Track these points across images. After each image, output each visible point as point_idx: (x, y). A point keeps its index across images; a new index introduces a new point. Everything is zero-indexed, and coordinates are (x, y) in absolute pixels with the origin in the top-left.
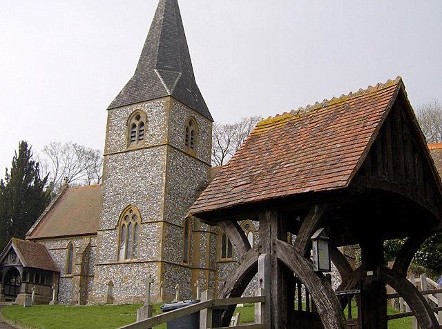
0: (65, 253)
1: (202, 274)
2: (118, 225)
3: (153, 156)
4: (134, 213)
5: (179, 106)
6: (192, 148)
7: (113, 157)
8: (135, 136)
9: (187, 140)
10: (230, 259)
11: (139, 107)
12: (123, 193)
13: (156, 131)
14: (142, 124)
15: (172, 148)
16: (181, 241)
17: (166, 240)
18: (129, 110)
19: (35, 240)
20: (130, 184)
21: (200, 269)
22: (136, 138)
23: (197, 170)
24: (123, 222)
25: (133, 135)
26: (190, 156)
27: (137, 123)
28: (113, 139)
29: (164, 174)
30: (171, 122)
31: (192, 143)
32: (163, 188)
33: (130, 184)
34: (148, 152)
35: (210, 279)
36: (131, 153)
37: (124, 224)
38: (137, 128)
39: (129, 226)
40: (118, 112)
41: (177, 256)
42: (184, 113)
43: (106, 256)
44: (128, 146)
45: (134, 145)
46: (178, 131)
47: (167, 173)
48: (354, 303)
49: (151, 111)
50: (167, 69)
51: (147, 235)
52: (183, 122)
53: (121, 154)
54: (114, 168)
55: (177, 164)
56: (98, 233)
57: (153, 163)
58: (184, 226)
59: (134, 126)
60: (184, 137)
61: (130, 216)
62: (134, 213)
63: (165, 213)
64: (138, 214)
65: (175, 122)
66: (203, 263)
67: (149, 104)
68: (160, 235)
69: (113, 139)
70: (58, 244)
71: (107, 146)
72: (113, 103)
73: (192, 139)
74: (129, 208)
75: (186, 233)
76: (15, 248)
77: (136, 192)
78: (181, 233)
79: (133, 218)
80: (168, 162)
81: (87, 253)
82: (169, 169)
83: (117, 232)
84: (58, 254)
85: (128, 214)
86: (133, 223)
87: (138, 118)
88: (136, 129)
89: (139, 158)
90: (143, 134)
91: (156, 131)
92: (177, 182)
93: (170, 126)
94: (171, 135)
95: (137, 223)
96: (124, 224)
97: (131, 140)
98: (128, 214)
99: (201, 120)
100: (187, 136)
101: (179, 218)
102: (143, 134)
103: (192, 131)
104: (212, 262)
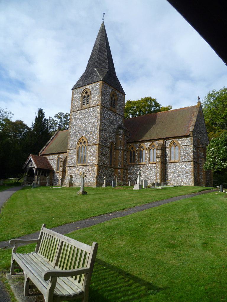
0: (56, 161)
1: (119, 171)
2: (77, 147)
3: (93, 111)
4: (84, 140)
5: (107, 86)
6: (114, 108)
7: (75, 113)
8: (85, 102)
9: (111, 104)
10: (134, 163)
11: (87, 87)
12: (79, 130)
13: (95, 99)
14: (88, 96)
15: (103, 107)
16: (108, 154)
17: (101, 154)
18: (82, 89)
19: (43, 155)
20: (82, 126)
22: (85, 103)
24: (79, 145)
25: (84, 101)
26: (113, 111)
27: (86, 96)
28: (75, 104)
29: (99, 120)
30: (103, 94)
31: (114, 105)
32: (99, 127)
33: (82, 126)
34: (91, 109)
35: (123, 174)
36: (83, 111)
38: (86, 98)
40: (77, 90)
41: (107, 162)
42: (110, 90)
43: (71, 162)
44: (82, 107)
45: (84, 106)
47: (100, 119)
48: (83, 275)
49: (93, 89)
50: (101, 68)
51: (90, 151)
53: (78, 111)
54: (75, 118)
55: (106, 115)
56: (68, 151)
57: (94, 115)
59: (85, 97)
60: (110, 102)
61: (83, 142)
62: (84, 140)
63: (99, 140)
64: (86, 141)
65: (105, 94)
66: (120, 166)
68: (97, 151)
69: (75, 104)
70: (53, 157)
71: (72, 108)
72: (75, 86)
73: (114, 103)
74: (82, 138)
75: (111, 150)
76: (32, 159)
77: (85, 130)
78: (108, 151)
79: (84, 143)
80: (101, 114)
81: (65, 161)
82: (102, 117)
83: (76, 150)
84: (53, 161)
85: (81, 141)
86: (84, 145)
87: (86, 93)
88: (86, 99)
89: (87, 113)
90: (89, 101)
91: (95, 99)
93: (102, 96)
94: (102, 100)
97: (83, 104)
99: (119, 94)
100: (111, 101)
101: (107, 143)
102: (89, 101)
103: (114, 100)
104: (125, 165)
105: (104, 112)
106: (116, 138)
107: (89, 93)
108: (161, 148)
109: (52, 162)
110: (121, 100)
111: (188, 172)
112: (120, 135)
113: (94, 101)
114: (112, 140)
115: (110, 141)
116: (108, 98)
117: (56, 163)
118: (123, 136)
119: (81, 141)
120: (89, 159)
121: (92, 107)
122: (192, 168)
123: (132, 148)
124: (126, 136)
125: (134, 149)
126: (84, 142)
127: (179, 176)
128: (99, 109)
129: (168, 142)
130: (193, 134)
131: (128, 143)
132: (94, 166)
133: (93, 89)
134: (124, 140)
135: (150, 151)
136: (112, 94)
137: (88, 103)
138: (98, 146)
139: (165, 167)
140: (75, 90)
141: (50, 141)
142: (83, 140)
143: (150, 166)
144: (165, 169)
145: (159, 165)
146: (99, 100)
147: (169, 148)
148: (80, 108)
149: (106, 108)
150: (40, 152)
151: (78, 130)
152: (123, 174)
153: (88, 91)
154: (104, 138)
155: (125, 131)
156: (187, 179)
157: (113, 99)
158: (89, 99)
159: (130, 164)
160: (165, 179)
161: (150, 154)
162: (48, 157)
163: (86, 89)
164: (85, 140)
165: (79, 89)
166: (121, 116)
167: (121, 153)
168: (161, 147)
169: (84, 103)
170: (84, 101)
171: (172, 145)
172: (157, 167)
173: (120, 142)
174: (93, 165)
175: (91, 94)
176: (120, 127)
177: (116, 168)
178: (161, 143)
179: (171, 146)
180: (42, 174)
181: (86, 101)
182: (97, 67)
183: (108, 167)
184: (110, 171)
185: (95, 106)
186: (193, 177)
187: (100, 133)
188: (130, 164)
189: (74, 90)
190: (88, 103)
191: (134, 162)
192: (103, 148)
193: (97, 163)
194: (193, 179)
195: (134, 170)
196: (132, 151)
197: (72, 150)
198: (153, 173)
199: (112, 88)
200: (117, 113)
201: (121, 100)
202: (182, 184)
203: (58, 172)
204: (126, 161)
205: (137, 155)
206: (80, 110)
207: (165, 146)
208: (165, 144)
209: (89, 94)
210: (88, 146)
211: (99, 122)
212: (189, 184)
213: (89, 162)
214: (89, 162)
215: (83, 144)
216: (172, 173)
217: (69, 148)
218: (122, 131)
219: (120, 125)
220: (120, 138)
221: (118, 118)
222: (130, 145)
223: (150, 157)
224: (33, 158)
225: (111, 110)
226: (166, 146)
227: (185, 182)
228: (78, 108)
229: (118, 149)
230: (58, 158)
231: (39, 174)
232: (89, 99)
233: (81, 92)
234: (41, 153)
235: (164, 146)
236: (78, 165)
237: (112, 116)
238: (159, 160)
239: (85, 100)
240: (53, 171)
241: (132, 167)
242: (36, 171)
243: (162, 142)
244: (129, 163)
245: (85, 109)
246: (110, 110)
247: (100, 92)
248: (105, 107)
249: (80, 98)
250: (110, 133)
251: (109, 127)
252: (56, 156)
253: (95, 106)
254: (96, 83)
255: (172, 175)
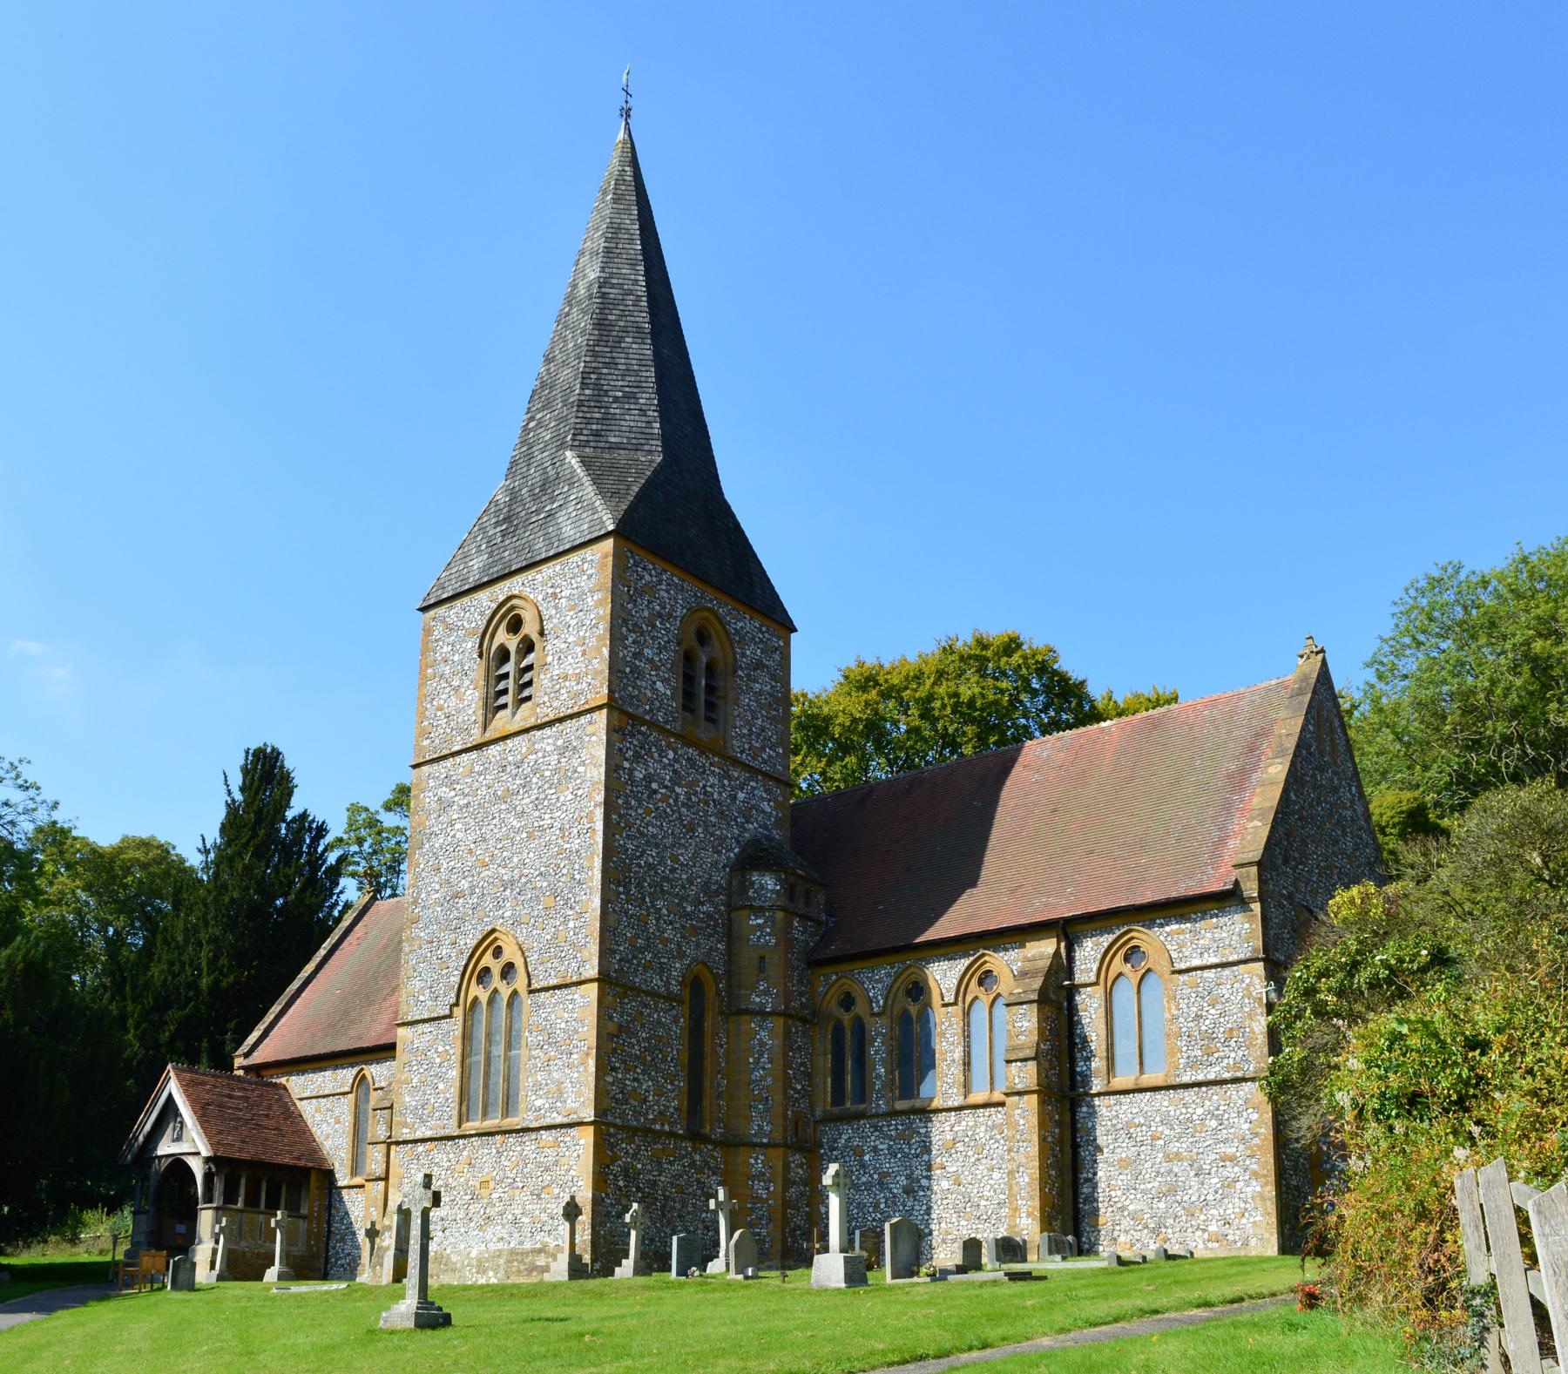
1: (757, 1162)
4: (507, 956)
5: (650, 572)
6: (714, 721)
8: (505, 692)
11: (514, 585)
12: (472, 888)
14: (528, 646)
16: (677, 1049)
18: (486, 601)
21: (755, 1145)
22: (508, 699)
23: (734, 798)
24: (476, 990)
25: (501, 686)
26: (703, 749)
27: (512, 643)
28: (440, 708)
30: (621, 624)
31: (710, 706)
34: (547, 740)
35: (787, 1183)
36: (494, 750)
37: (476, 998)
39: (491, 1001)
40: (451, 613)
44: (485, 728)
45: (503, 722)
46: (651, 661)
47: (609, 806)
52: (668, 631)
54: (445, 805)
55: (649, 778)
58: (687, 996)
59: (503, 655)
60: (677, 682)
61: (496, 967)
62: (507, 956)
63: (605, 953)
64: (519, 963)
65: (636, 628)
66: (759, 1125)
67: (547, 570)
69: (440, 708)
73: (710, 689)
74: (489, 942)
77: (512, 882)
83: (455, 1026)
86: (505, 992)
87: (515, 625)
88: (509, 667)
90: (529, 683)
91: (571, 665)
92: (652, 842)
94: (618, 672)
95: (515, 993)
96: (476, 998)
97: (492, 707)
98: (488, 960)
100: (689, 679)
101: (661, 970)
103: (710, 668)
105: (637, 757)
106: (730, 934)
107: (530, 628)
108: (1043, 992)
109: (318, 1117)
110: (759, 665)
111: (1232, 1159)
112: (759, 911)
113: (566, 678)
114: (698, 945)
115: (682, 955)
116: (659, 653)
117: (348, 1119)
118: (780, 915)
119: (488, 960)
120: (538, 1087)
121: (550, 724)
122: (1260, 1123)
123: (847, 1002)
124: (804, 918)
125: (860, 1009)
126: (508, 971)
127: (1172, 1191)
128: (595, 731)
129: (1089, 952)
130: (1262, 881)
131: (816, 961)
132: (574, 1132)
133: (554, 594)
134: (787, 942)
135: (967, 1014)
136: (692, 629)
137: (526, 693)
138: (592, 990)
139: (1074, 1122)
140: (441, 610)
141: (309, 968)
142: (498, 952)
143: (968, 1118)
144: (1074, 1137)
145: (1026, 1113)
146: (597, 673)
147: (1100, 990)
148: (476, 736)
149: (653, 725)
150: (245, 1048)
151: (464, 884)
152: (785, 1189)
153: (528, 616)
154: (636, 936)
155: (792, 879)
156: (1232, 1208)
157: (704, 660)
158: (530, 668)
159: (836, 1110)
160: (1076, 1211)
161: (967, 1036)
162: (297, 1085)
163: (514, 602)
164: (510, 953)
165: (465, 600)
166: (766, 775)
167: (767, 1035)
168: (1037, 983)
169: (502, 700)
170: (501, 686)
171: (1118, 964)
172: (1014, 1126)
173: (762, 959)
174: (562, 1126)
175: (542, 633)
176: (755, 857)
177: (734, 1143)
178: (1042, 957)
179: (1112, 976)
180: (252, 1201)
181: (510, 684)
182: (586, 444)
183: (672, 1134)
184: (693, 1164)
185: (571, 717)
186: (1270, 1191)
187: (605, 902)
188: (836, 1110)
189: (432, 613)
190: (526, 693)
191: (861, 1094)
192: (632, 1005)
193: (589, 1114)
194: (1272, 1207)
195: (862, 1154)
196: (847, 1018)
197: (426, 1027)
198: (992, 1169)
199: (693, 587)
200: (736, 762)
201: (759, 665)
202: (1201, 1247)
203: (358, 1180)
204: (804, 1094)
205: (877, 1049)
206: (478, 747)
207: (1070, 974)
208: (1071, 959)
209: (535, 637)
210: (530, 992)
211: (599, 826)
212: (1246, 1244)
213: (538, 1103)
214: (534, 1105)
215: (496, 981)
216: (1124, 1164)
217: (406, 1014)
218: (770, 882)
219: (755, 843)
220: (759, 930)
221: (741, 796)
222: (829, 984)
223: (967, 1064)
224: (187, 1088)
225: (687, 741)
226: (1079, 978)
227: (1213, 1228)
228: (461, 731)
229: (747, 1012)
230: (361, 1080)
231: (230, 1197)
232: (530, 668)
233: (482, 624)
234: (247, 1055)
235: (1062, 975)
236: (471, 1126)
237: (694, 783)
238: (1027, 1075)
239: (506, 676)
240: (329, 1175)
241: (847, 1132)
242: (208, 1177)
243: (1045, 948)
244: (824, 1101)
245: (504, 738)
246: (678, 736)
247: (599, 618)
248: (644, 722)
249: (477, 669)
250: (684, 898)
251: (675, 859)
252: (347, 1075)
253: (571, 717)
254: (575, 558)
255: (1124, 1179)
